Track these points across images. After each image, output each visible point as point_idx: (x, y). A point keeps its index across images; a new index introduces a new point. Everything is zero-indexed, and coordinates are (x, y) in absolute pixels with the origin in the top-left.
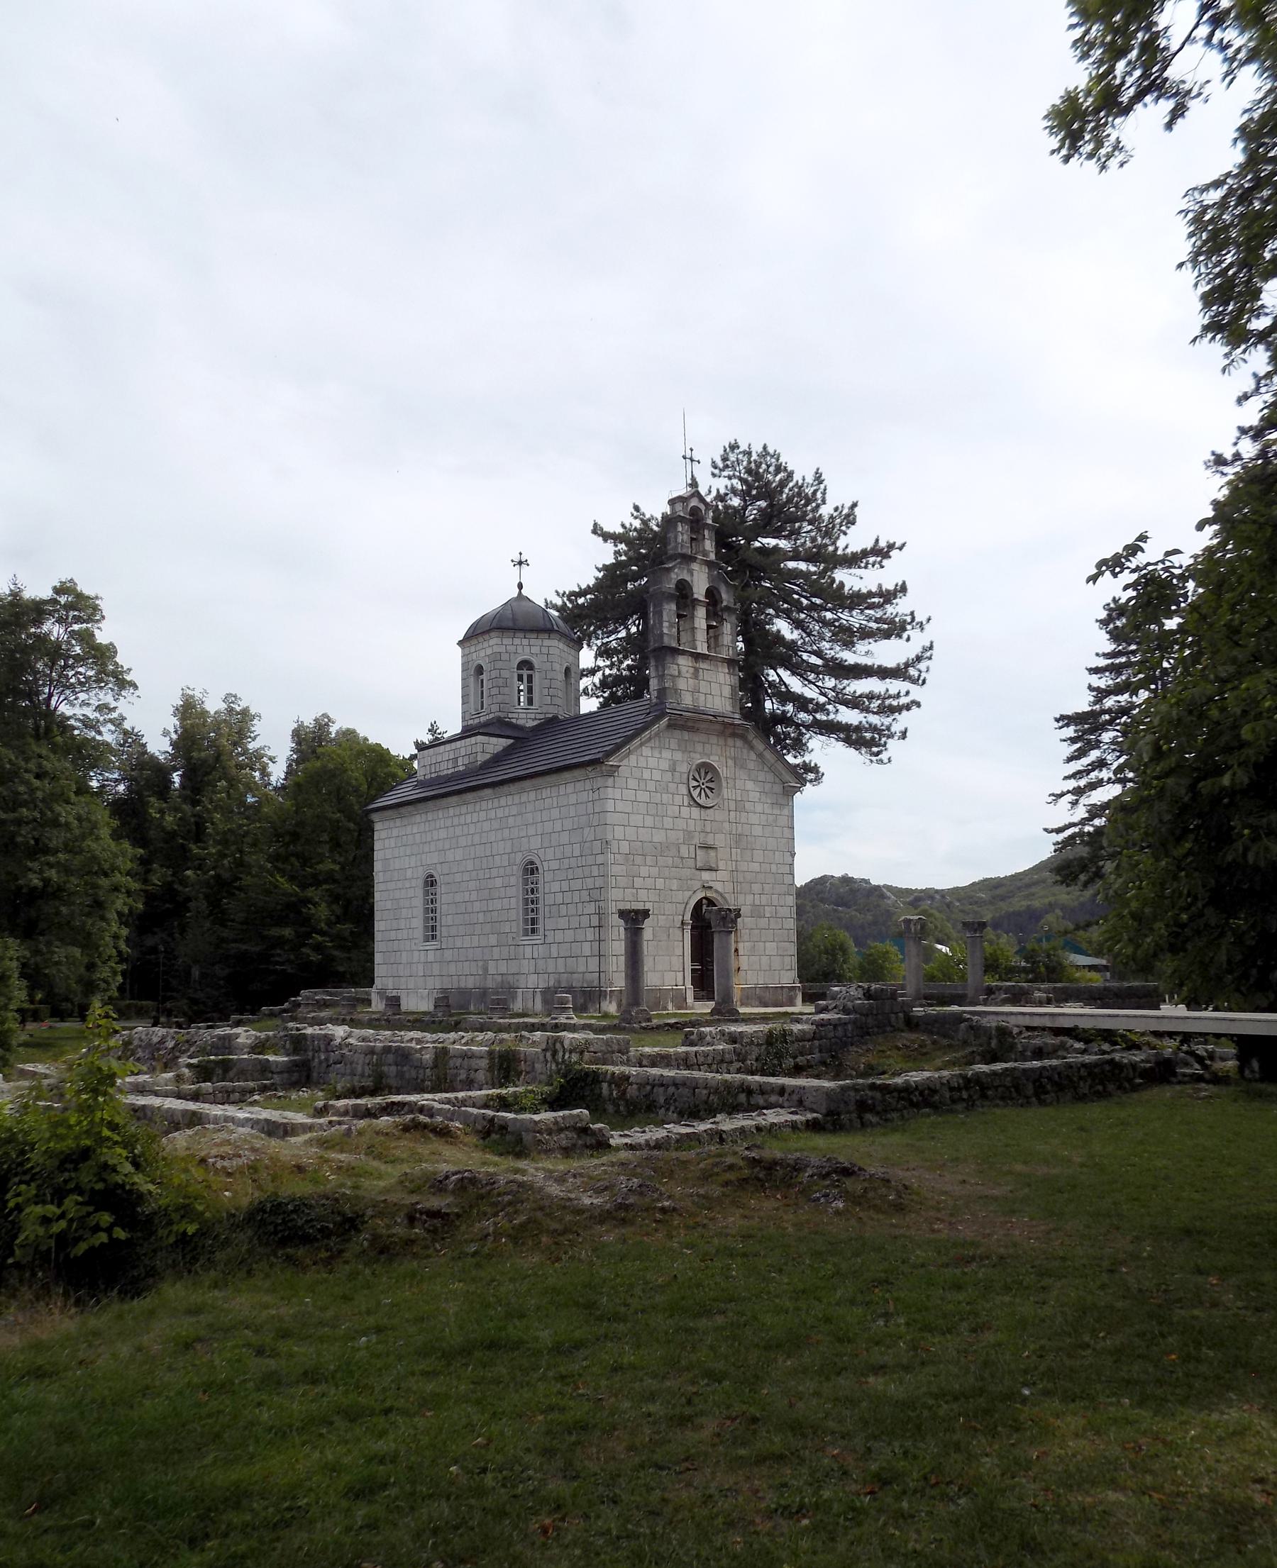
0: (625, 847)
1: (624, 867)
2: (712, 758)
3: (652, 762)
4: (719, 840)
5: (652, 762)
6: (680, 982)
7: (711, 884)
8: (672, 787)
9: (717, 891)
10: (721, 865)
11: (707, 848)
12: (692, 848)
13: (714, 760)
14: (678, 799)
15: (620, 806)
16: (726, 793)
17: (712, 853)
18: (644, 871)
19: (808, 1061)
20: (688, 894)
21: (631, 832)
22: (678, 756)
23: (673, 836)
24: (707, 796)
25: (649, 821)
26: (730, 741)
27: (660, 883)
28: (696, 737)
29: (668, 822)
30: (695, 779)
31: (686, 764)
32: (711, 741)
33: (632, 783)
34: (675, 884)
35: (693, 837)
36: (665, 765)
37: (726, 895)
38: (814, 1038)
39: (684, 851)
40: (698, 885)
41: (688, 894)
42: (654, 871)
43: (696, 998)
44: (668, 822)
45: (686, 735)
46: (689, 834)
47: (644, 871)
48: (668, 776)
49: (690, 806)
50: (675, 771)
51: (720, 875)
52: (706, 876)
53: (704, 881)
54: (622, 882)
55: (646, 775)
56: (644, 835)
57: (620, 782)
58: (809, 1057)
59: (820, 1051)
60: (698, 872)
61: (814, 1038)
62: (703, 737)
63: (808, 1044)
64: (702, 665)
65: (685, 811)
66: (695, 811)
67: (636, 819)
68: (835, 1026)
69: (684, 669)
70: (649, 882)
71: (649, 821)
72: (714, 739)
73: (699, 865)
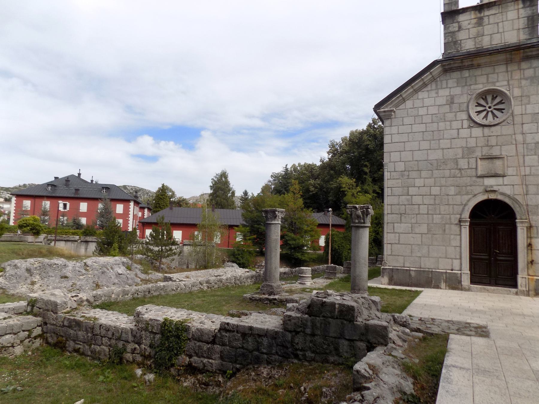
0: (401, 167)
1: (400, 181)
2: (497, 84)
3: (427, 102)
4: (508, 150)
5: (427, 102)
6: (458, 268)
7: (495, 188)
8: (450, 116)
9: (502, 194)
10: (510, 171)
11: (491, 158)
12: (473, 161)
13: (501, 86)
14: (456, 125)
15: (396, 138)
16: (517, 109)
17: (498, 163)
18: (419, 182)
19: (204, 365)
20: (466, 198)
21: (407, 156)
22: (457, 91)
23: (450, 154)
24: (494, 116)
25: (425, 145)
26: (524, 65)
27: (435, 190)
28: (478, 72)
29: (445, 143)
30: (479, 105)
31: (465, 96)
32: (497, 71)
33: (407, 121)
34: (452, 191)
35: (474, 152)
36: (442, 101)
37: (516, 197)
38: (213, 342)
39: (463, 164)
40: (481, 189)
41: (466, 198)
42: (431, 181)
43: (473, 282)
44: (445, 143)
45: (466, 73)
46: (468, 151)
47: (419, 182)
48: (447, 108)
49: (470, 127)
50: (452, 103)
51: (506, 180)
52: (490, 182)
53: (487, 186)
54: (397, 191)
55: (422, 111)
56: (419, 155)
57: (395, 122)
58: (205, 360)
59: (222, 358)
60: (480, 180)
61: (213, 342)
62: (488, 70)
63: (205, 347)
64: (487, 13)
65: (465, 133)
66: (477, 132)
67: (414, 145)
68: (244, 335)
69: (465, 24)
70: (424, 190)
71: (425, 145)
72: (502, 68)
73: (480, 173)
